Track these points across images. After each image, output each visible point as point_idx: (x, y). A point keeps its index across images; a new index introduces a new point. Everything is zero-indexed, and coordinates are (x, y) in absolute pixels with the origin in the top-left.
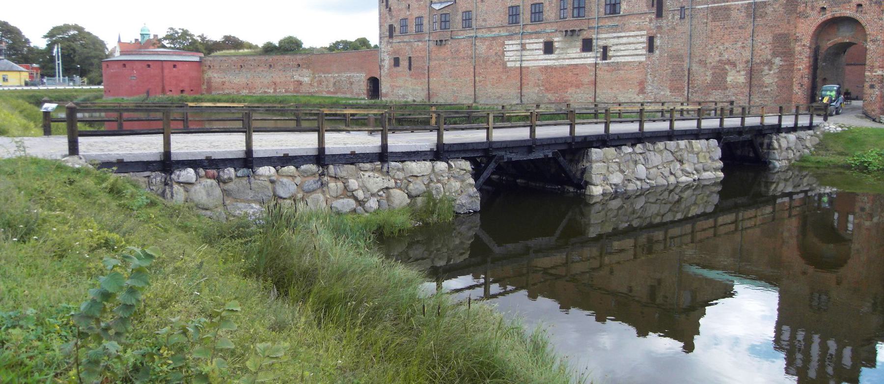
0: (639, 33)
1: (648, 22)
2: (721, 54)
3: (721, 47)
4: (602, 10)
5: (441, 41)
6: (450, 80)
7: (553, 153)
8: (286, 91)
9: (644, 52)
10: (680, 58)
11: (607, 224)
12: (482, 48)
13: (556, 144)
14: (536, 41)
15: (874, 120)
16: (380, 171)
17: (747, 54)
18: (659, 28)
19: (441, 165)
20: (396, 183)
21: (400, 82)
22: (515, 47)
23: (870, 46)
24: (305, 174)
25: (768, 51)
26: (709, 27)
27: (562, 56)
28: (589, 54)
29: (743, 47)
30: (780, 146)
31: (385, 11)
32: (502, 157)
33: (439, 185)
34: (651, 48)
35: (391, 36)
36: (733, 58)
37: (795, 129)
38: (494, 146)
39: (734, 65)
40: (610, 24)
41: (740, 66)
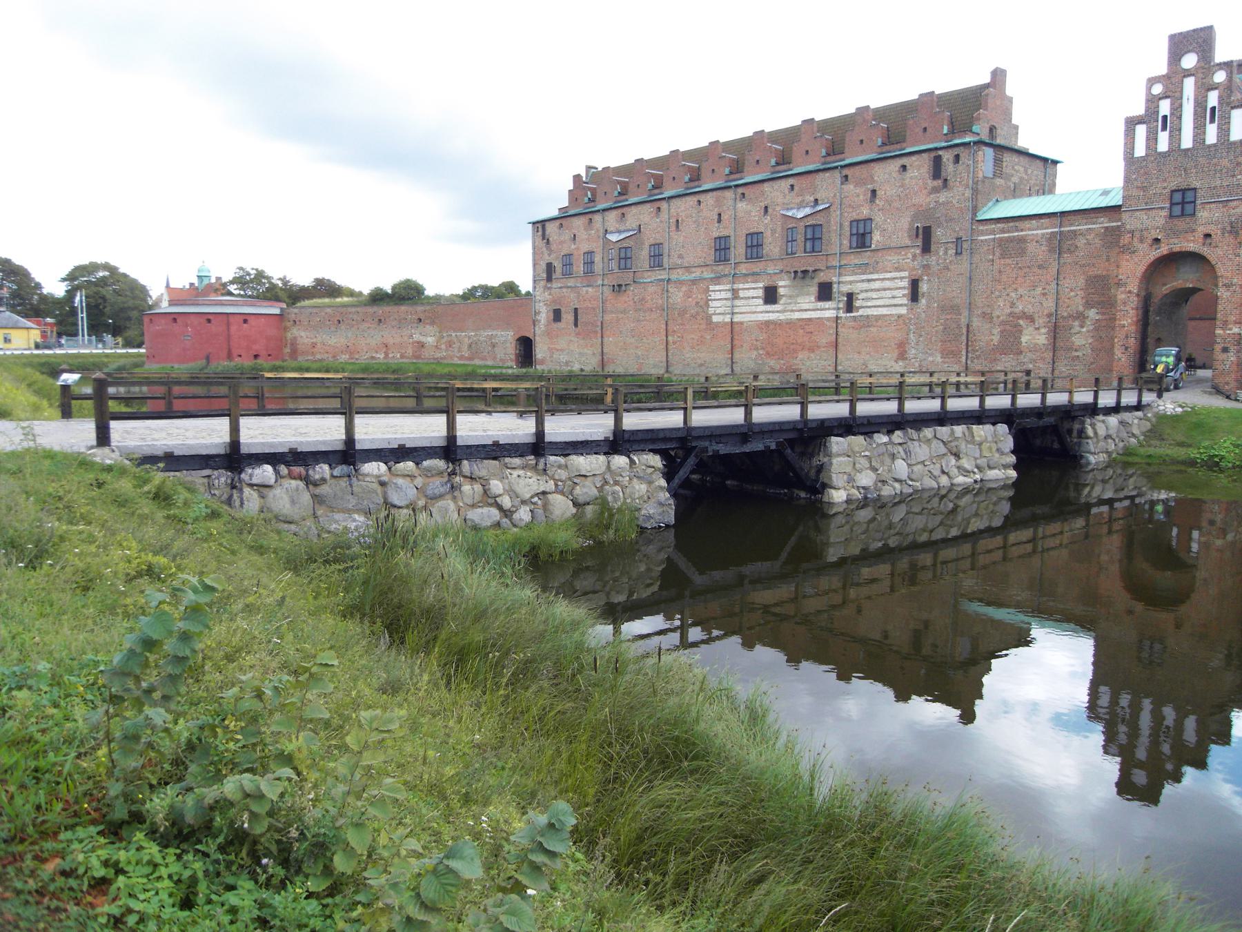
1: (911, 259)
2: (1013, 305)
3: (1013, 295)
4: (846, 242)
5: (620, 286)
6: (633, 340)
7: (778, 444)
8: (402, 356)
9: (905, 301)
10: (955, 309)
11: (853, 543)
12: (677, 296)
13: (781, 431)
14: (753, 285)
15: (1228, 397)
16: (535, 468)
17: (1049, 304)
18: (926, 267)
19: (620, 461)
20: (556, 485)
21: (562, 343)
22: (723, 295)
23: (1223, 293)
24: (428, 474)
26: (996, 267)
27: (790, 308)
28: (827, 304)
29: (1044, 294)
30: (1096, 433)
31: (541, 244)
32: (705, 450)
33: (617, 488)
34: (914, 296)
35: (549, 279)
36: (1029, 309)
37: (1116, 409)
38: (694, 434)
39: (1031, 319)
40: (856, 261)
41: (1040, 321)
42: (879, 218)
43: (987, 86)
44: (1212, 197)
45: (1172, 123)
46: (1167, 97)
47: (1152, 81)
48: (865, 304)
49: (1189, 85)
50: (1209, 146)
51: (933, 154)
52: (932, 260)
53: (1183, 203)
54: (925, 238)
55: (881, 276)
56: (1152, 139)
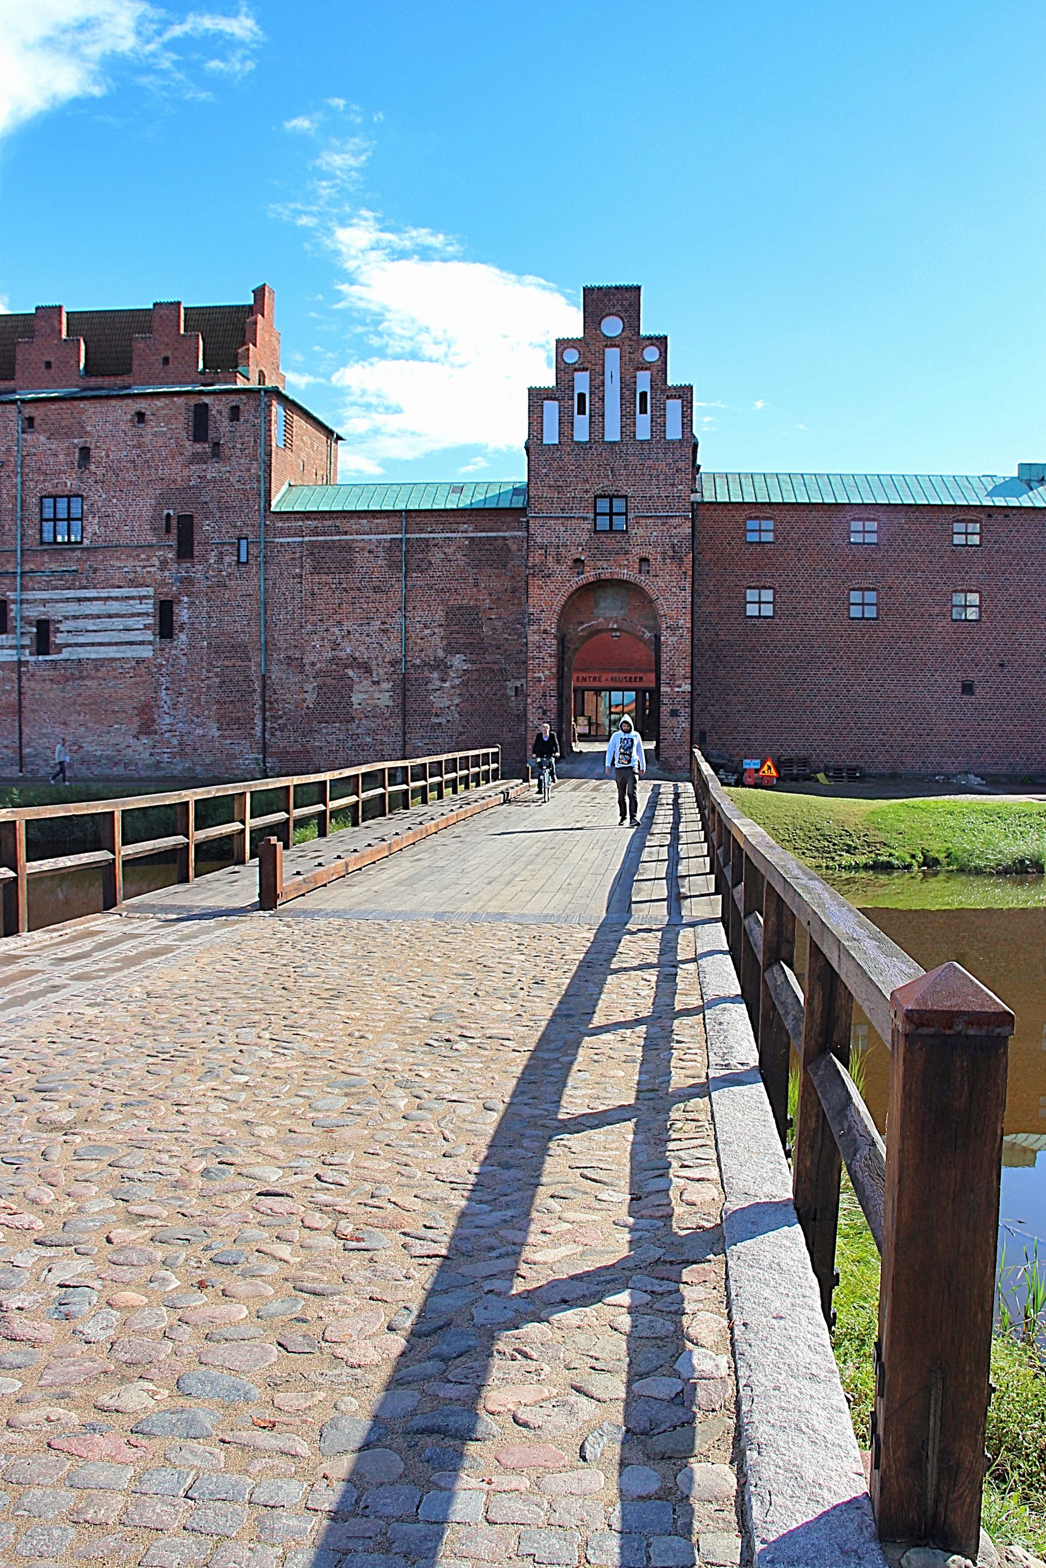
0: (134, 592)
1: (158, 566)
2: (335, 646)
3: (336, 630)
9: (149, 636)
10: (240, 651)
18: (187, 581)
25: (436, 640)
36: (363, 653)
40: (54, 566)
41: (380, 672)
42: (96, 496)
44: (649, 509)
45: (591, 405)
46: (585, 369)
47: (562, 344)
48: (72, 640)
49: (613, 356)
50: (642, 442)
51: (194, 401)
52: (198, 570)
53: (609, 515)
54: (183, 536)
55: (104, 594)
56: (566, 423)
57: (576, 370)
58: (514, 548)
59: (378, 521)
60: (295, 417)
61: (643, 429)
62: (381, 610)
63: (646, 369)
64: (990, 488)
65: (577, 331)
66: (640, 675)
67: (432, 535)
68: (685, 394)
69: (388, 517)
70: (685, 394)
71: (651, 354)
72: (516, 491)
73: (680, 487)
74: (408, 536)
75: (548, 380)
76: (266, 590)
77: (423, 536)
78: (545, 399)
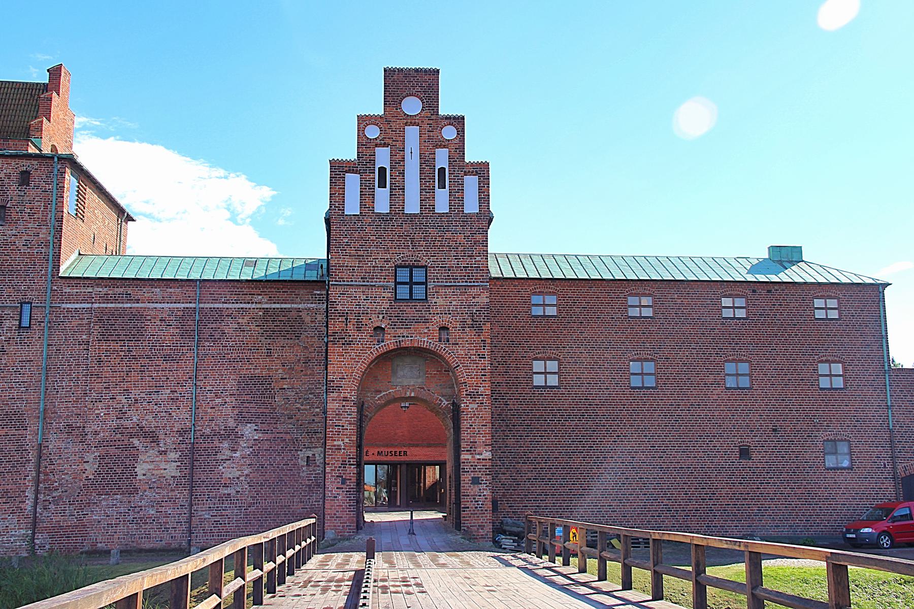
2: (121, 415)
26: (92, 353)
36: (149, 421)
43: (45, 88)
44: (448, 278)
47: (364, 121)
49: (412, 135)
50: (441, 215)
53: (410, 281)
56: (367, 195)
57: (376, 145)
58: (308, 319)
59: (171, 290)
60: (88, 189)
61: (442, 201)
62: (171, 378)
63: (444, 147)
64: (748, 267)
65: (378, 109)
66: (405, 449)
67: (225, 306)
68: (482, 171)
69: (182, 287)
70: (482, 171)
71: (449, 133)
72: (308, 267)
73: (478, 258)
74: (202, 305)
75: (351, 154)
76: (49, 356)
77: (216, 306)
78: (346, 172)
